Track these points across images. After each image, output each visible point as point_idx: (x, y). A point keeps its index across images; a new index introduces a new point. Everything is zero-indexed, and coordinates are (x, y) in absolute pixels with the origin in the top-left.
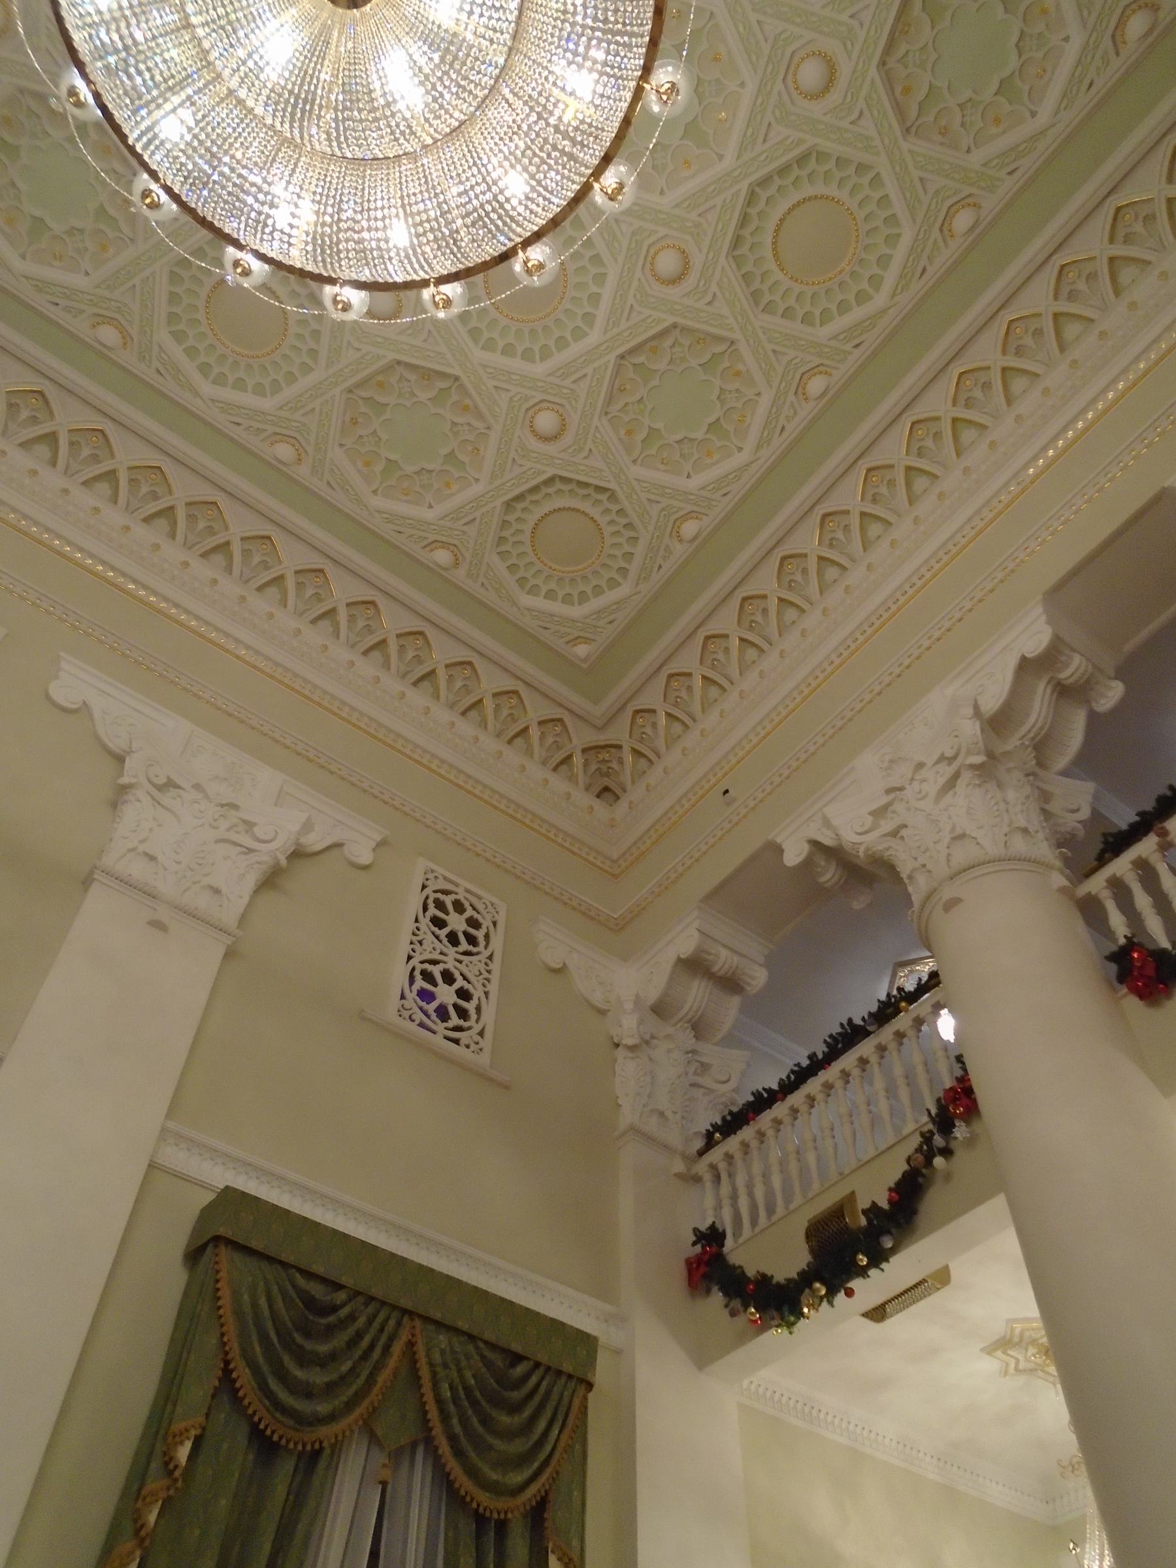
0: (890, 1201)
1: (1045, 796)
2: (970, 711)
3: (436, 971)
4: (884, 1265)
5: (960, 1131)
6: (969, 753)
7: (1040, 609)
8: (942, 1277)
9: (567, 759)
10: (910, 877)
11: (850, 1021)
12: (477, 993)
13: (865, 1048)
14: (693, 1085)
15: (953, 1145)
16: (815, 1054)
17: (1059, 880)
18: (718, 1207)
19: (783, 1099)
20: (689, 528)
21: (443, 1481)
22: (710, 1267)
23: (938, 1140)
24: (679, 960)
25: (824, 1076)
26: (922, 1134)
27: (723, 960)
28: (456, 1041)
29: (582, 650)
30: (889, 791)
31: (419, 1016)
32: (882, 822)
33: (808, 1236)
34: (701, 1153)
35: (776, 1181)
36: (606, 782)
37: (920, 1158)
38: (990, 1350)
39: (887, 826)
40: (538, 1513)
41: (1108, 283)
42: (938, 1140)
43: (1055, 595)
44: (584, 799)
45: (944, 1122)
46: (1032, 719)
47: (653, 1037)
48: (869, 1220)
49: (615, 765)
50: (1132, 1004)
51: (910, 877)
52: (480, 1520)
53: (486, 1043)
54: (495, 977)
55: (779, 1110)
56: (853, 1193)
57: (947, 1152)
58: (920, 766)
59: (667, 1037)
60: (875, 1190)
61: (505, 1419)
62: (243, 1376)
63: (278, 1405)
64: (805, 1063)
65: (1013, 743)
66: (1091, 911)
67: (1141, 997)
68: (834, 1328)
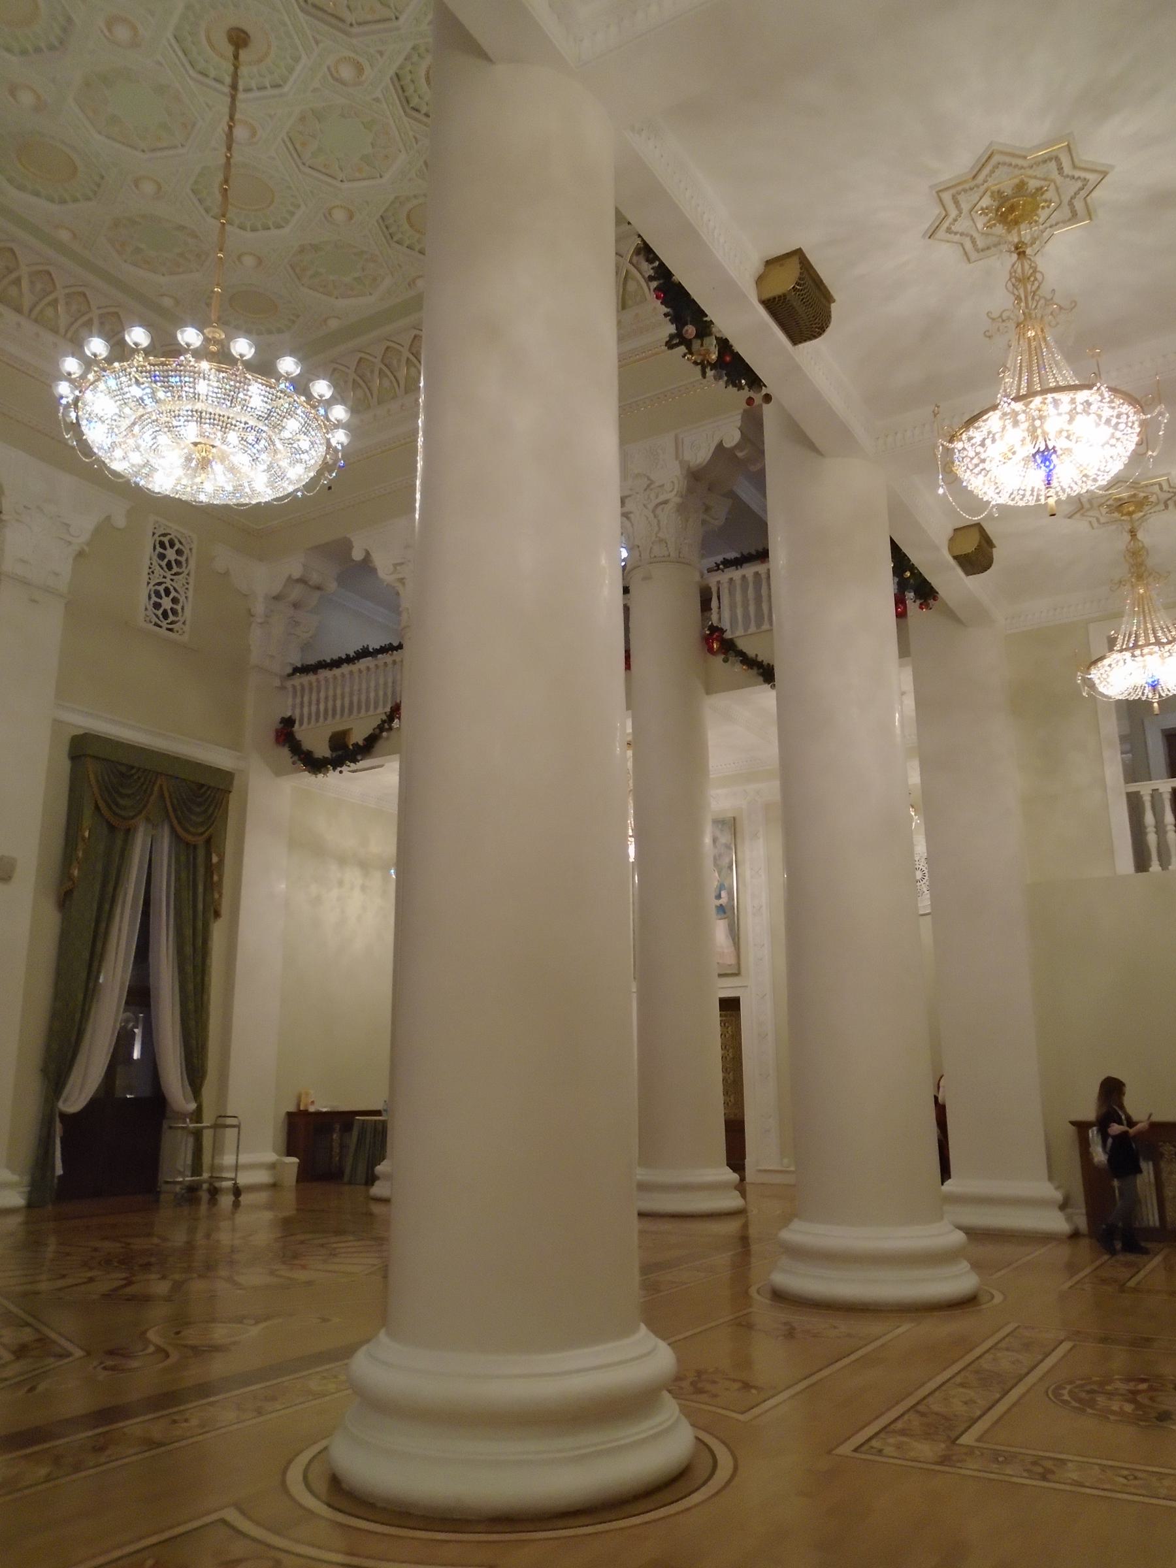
3: (161, 589)
8: (382, 766)
12: (182, 599)
18: (294, 706)
21: (173, 830)
22: (286, 733)
23: (386, 726)
27: (315, 578)
28: (170, 630)
31: (155, 619)
34: (289, 675)
37: (377, 731)
40: (208, 841)
42: (386, 726)
52: (187, 844)
53: (187, 628)
54: (191, 587)
60: (358, 737)
61: (198, 810)
62: (101, 804)
63: (115, 814)
68: (332, 779)
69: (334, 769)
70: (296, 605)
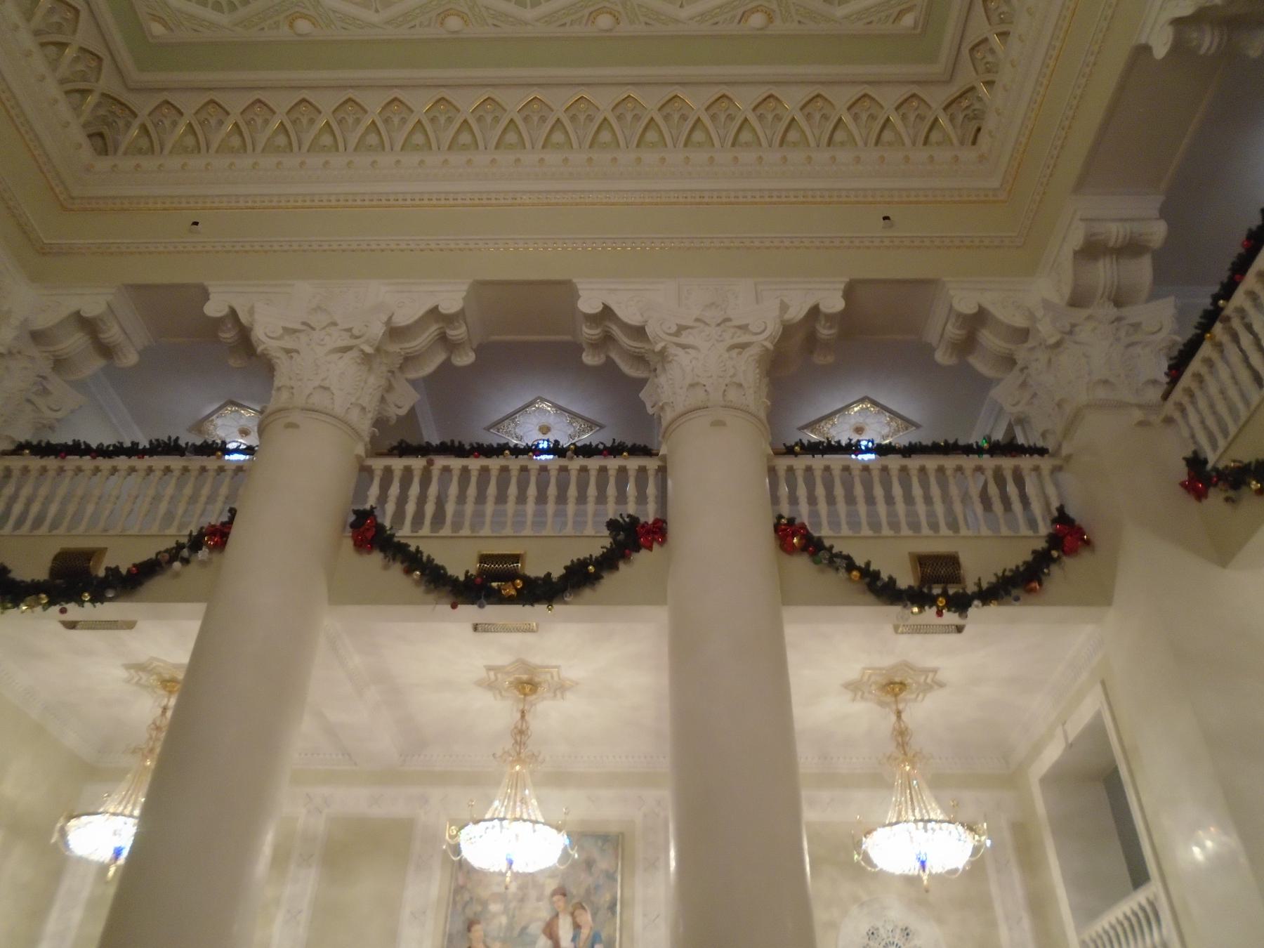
0: (129, 571)
1: (389, 388)
2: (385, 319)
4: (98, 604)
5: (203, 554)
6: (367, 342)
7: (465, 287)
8: (130, 625)
9: (84, 92)
10: (279, 389)
11: (177, 439)
13: (175, 462)
14: (29, 401)
15: (193, 558)
16: (138, 444)
17: (360, 450)
19: (94, 458)
20: (303, 26)
23: (185, 553)
24: (78, 312)
25: (134, 461)
26: (177, 543)
27: (112, 333)
29: (157, 29)
30: (304, 323)
32: (286, 337)
33: (56, 558)
35: (53, 509)
36: (105, 130)
37: (167, 556)
38: (128, 667)
39: (288, 343)
41: (641, 130)
42: (185, 553)
43: (481, 287)
44: (79, 136)
45: (196, 543)
46: (413, 344)
47: (19, 353)
48: (106, 576)
49: (121, 123)
50: (349, 543)
51: (279, 389)
55: (87, 462)
56: (106, 549)
57: (186, 561)
58: (334, 324)
59: (32, 359)
60: (122, 558)
64: (127, 444)
65: (394, 348)
66: (365, 472)
67: (355, 544)
69: (52, 603)
70: (60, 364)
